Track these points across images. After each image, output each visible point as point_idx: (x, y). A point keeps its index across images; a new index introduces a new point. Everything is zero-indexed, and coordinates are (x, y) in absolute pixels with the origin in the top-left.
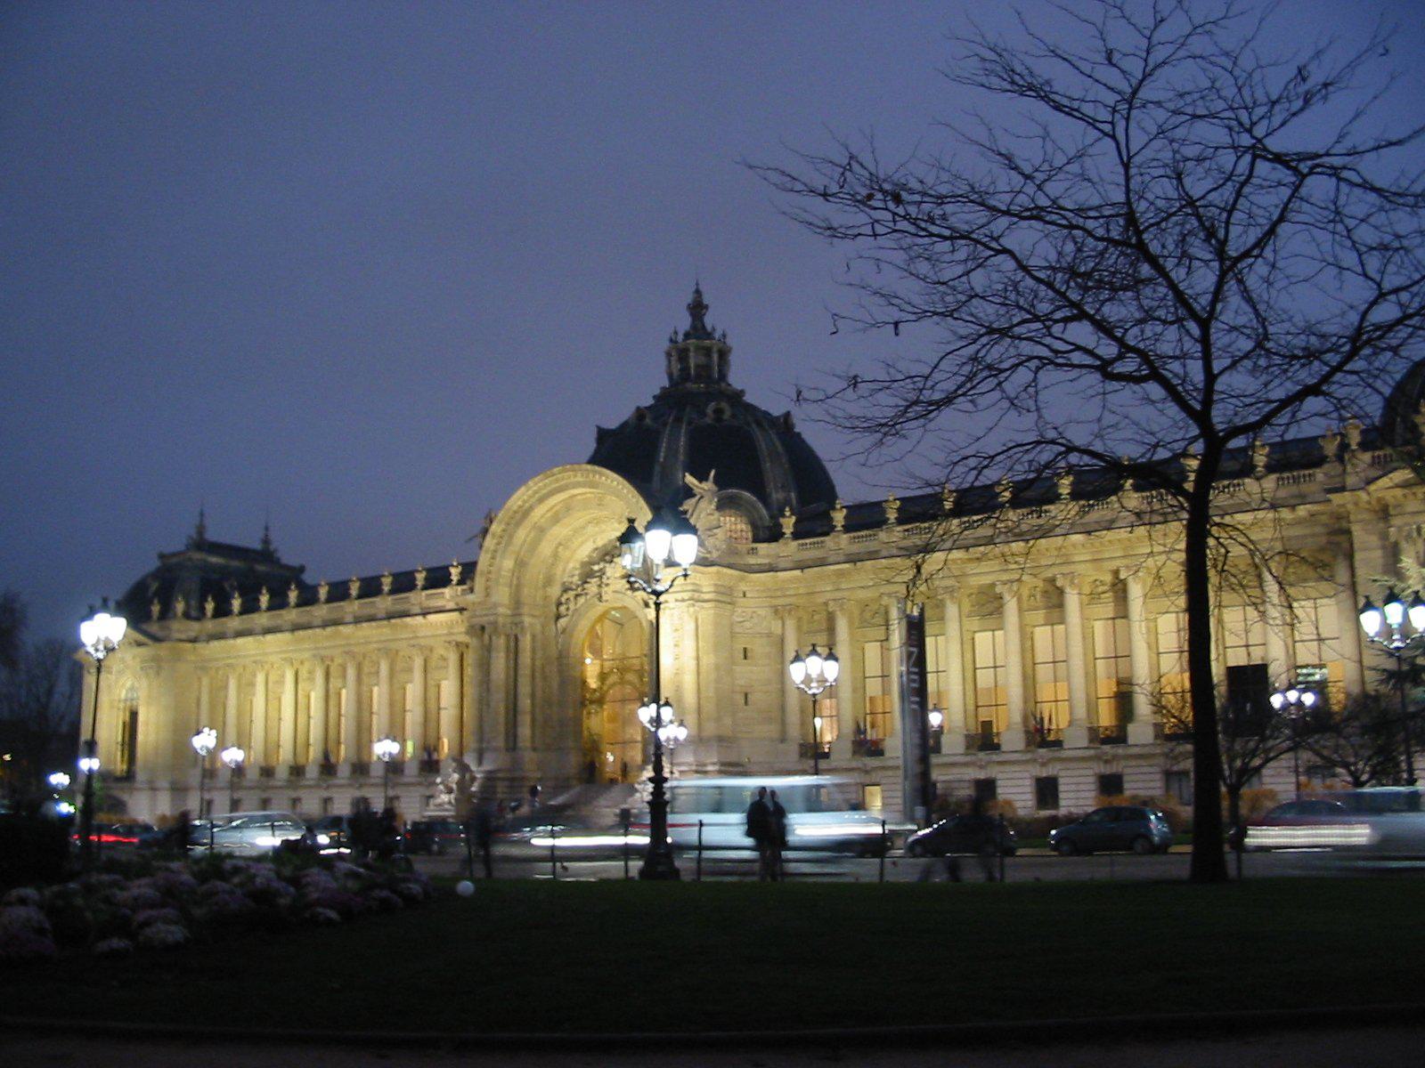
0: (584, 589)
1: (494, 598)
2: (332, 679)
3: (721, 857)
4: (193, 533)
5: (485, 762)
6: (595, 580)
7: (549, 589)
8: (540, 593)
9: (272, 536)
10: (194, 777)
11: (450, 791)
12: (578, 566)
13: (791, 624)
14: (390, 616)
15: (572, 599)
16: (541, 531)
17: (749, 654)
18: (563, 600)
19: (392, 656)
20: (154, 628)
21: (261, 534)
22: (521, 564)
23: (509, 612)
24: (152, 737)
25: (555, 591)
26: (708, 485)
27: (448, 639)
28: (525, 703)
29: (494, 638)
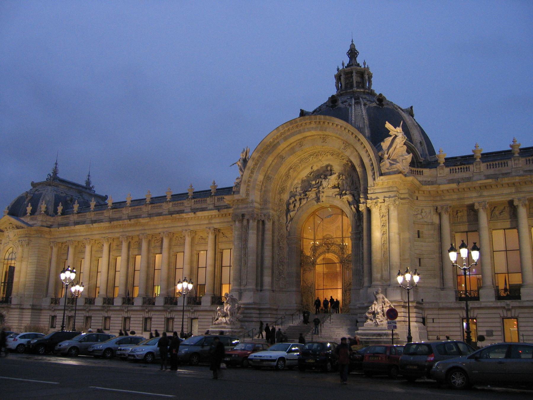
2: (131, 250)
6: (314, 189)
9: (91, 179)
10: (46, 302)
11: (225, 316)
12: (300, 182)
13: (446, 218)
14: (171, 213)
15: (298, 200)
17: (421, 235)
18: (291, 201)
19: (171, 236)
20: (27, 219)
21: (86, 178)
22: (268, 178)
23: (260, 207)
24: (22, 280)
25: (286, 197)
26: (399, 129)
28: (268, 261)
29: (251, 221)
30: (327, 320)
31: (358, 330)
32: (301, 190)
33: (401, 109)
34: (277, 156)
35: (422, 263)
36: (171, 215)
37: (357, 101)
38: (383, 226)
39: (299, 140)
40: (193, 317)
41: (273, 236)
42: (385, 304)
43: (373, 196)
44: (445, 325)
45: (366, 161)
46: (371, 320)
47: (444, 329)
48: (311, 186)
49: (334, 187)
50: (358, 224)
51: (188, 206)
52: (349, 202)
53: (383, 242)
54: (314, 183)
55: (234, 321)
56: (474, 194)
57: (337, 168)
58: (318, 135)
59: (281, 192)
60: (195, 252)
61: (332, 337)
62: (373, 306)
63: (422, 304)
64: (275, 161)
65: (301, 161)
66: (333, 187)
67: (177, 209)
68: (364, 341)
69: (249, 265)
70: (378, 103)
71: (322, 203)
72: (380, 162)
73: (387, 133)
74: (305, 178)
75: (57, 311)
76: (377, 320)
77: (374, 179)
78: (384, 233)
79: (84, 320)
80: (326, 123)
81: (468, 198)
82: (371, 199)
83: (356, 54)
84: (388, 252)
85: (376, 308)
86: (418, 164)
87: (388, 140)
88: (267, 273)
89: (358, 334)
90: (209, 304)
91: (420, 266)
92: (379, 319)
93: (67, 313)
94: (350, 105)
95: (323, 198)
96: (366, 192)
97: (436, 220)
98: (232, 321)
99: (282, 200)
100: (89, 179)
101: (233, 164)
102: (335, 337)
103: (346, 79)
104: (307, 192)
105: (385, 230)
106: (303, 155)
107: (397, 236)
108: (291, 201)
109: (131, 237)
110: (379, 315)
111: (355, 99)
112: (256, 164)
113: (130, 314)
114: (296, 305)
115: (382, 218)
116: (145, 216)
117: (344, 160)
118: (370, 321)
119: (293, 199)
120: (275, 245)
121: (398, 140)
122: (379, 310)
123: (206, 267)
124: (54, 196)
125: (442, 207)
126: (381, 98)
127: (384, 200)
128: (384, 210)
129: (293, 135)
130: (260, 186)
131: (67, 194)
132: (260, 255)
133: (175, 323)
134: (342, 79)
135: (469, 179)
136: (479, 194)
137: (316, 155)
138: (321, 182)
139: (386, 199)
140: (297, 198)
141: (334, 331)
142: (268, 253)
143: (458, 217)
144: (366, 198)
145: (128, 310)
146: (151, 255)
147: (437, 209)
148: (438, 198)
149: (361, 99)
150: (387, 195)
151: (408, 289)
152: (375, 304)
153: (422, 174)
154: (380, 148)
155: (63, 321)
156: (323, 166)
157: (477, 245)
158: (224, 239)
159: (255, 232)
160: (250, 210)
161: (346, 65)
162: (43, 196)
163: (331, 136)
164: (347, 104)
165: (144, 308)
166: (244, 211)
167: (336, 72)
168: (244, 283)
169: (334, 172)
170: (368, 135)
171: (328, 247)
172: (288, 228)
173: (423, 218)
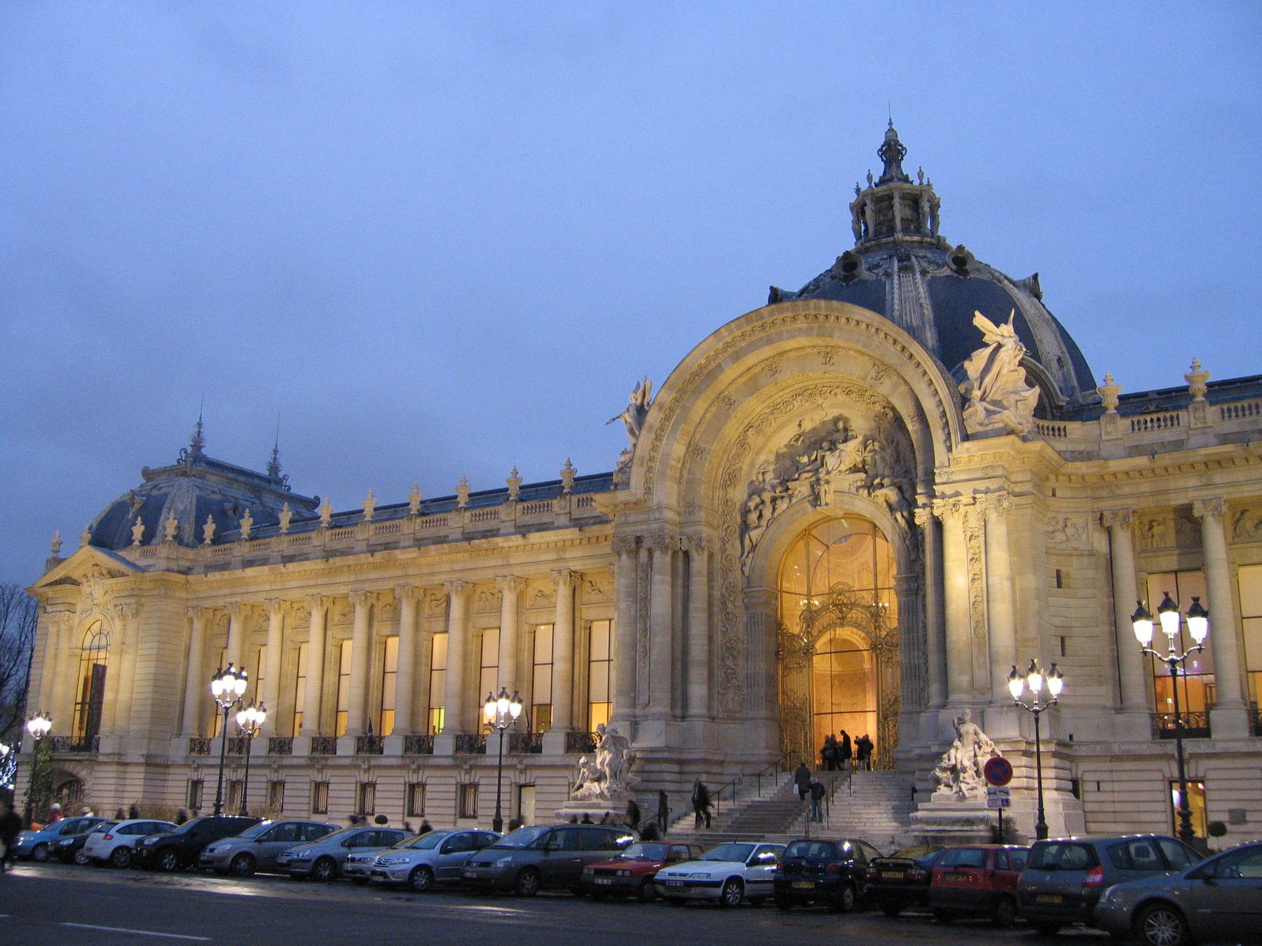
0: (788, 489)
1: (658, 497)
2: (376, 624)
3: (723, 864)
4: (187, 444)
5: (641, 734)
7: (730, 490)
8: (719, 494)
9: (282, 460)
10: (178, 750)
11: (599, 778)
12: (772, 458)
13: (1123, 540)
14: (468, 537)
15: (768, 501)
16: (727, 403)
18: (752, 505)
19: (470, 590)
20: (132, 554)
22: (695, 451)
23: (677, 518)
24: (124, 696)
25: (739, 494)
26: (1007, 329)
27: (557, 566)
28: (698, 649)
29: (657, 554)
30: (842, 787)
31: (917, 810)
32: (775, 478)
33: (1011, 282)
34: (718, 398)
35: (1068, 649)
36: (467, 542)
37: (905, 263)
38: (971, 560)
39: (767, 359)
40: (523, 782)
41: (710, 588)
42: (980, 747)
43: (948, 490)
44: (1127, 797)
45: (929, 405)
46: (948, 785)
47: (1128, 807)
48: (798, 467)
49: (854, 469)
50: (913, 557)
51: (508, 519)
52: (890, 506)
53: (973, 600)
54: (805, 459)
55: (619, 790)
56: (1193, 482)
57: (860, 423)
58: (814, 347)
59: (728, 482)
60: (526, 628)
61: (854, 827)
62: (952, 751)
63: (1071, 746)
64: (713, 409)
65: (775, 409)
66: (850, 469)
67: (482, 526)
68: (932, 837)
69: (654, 657)
70: (954, 267)
71: (825, 507)
72: (963, 408)
73: (978, 340)
74: (785, 450)
75: (204, 770)
76: (963, 786)
77: (950, 449)
78: (976, 577)
79: (267, 789)
80: (833, 317)
81: (1176, 490)
82: (943, 496)
83: (900, 152)
84: (986, 622)
85: (959, 756)
86: (1054, 411)
87: (981, 356)
88: (697, 675)
89: (918, 821)
90: (561, 751)
91: (1063, 655)
92: (968, 784)
93: (229, 774)
94: (888, 275)
95: (828, 496)
96: (930, 481)
97: (1099, 542)
98: (615, 791)
99: (730, 503)
100: (275, 459)
101: (614, 419)
102: (861, 829)
103: (878, 212)
104: (789, 483)
105: (977, 571)
106: (777, 396)
107: (1006, 584)
108: (752, 505)
109: (375, 594)
110: (966, 775)
111: (900, 260)
112: (667, 418)
113: (375, 777)
114: (767, 751)
115: (970, 541)
116: (407, 544)
117: (877, 405)
118: (946, 788)
119: (757, 500)
120: (716, 609)
121: (1003, 355)
122: (967, 763)
123: (552, 664)
124: (194, 500)
125: (1114, 514)
126: (961, 255)
127: (974, 498)
128: (974, 522)
129: (753, 347)
130: (677, 471)
131: (225, 495)
132: (679, 634)
133: (481, 796)
134: (869, 211)
135: (1178, 445)
136: (1205, 481)
137: (808, 393)
138: (824, 456)
139: (978, 496)
140: (767, 496)
141: (858, 813)
142: (698, 628)
143: (1153, 536)
144: (932, 495)
145: (369, 769)
146: (423, 635)
147: (1101, 518)
148: (1104, 493)
149: (913, 258)
150: (981, 485)
151: (1036, 712)
152: (957, 749)
153: (1065, 435)
154: (961, 376)
155: (219, 793)
156: (825, 419)
157: (1203, 604)
158: (594, 597)
159: (668, 578)
160: (656, 526)
161: (876, 179)
162: (169, 500)
163: (844, 348)
164: (880, 271)
165: (408, 761)
166: (640, 529)
167: (853, 198)
168: (643, 699)
169: (853, 433)
170: (933, 345)
171: (842, 612)
172: (746, 570)
173: (1068, 540)
